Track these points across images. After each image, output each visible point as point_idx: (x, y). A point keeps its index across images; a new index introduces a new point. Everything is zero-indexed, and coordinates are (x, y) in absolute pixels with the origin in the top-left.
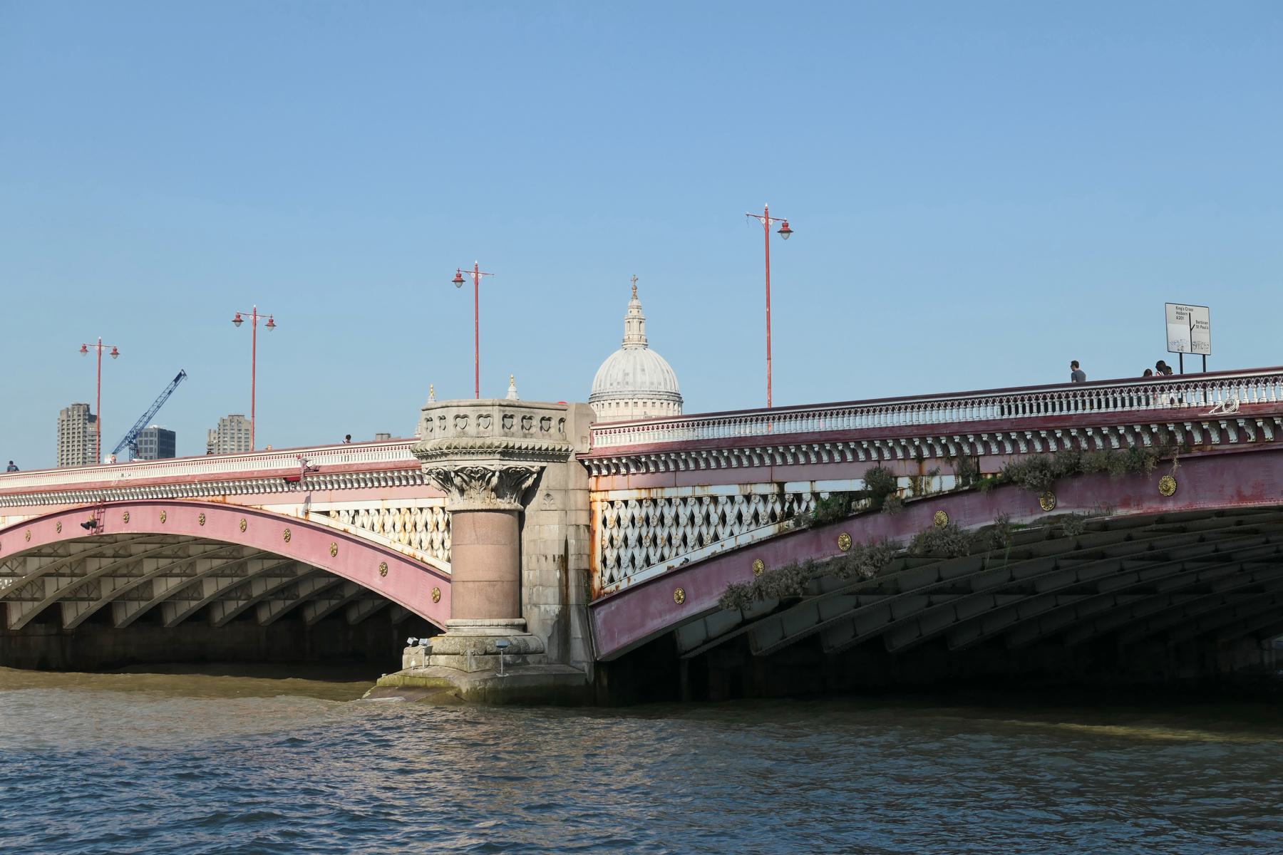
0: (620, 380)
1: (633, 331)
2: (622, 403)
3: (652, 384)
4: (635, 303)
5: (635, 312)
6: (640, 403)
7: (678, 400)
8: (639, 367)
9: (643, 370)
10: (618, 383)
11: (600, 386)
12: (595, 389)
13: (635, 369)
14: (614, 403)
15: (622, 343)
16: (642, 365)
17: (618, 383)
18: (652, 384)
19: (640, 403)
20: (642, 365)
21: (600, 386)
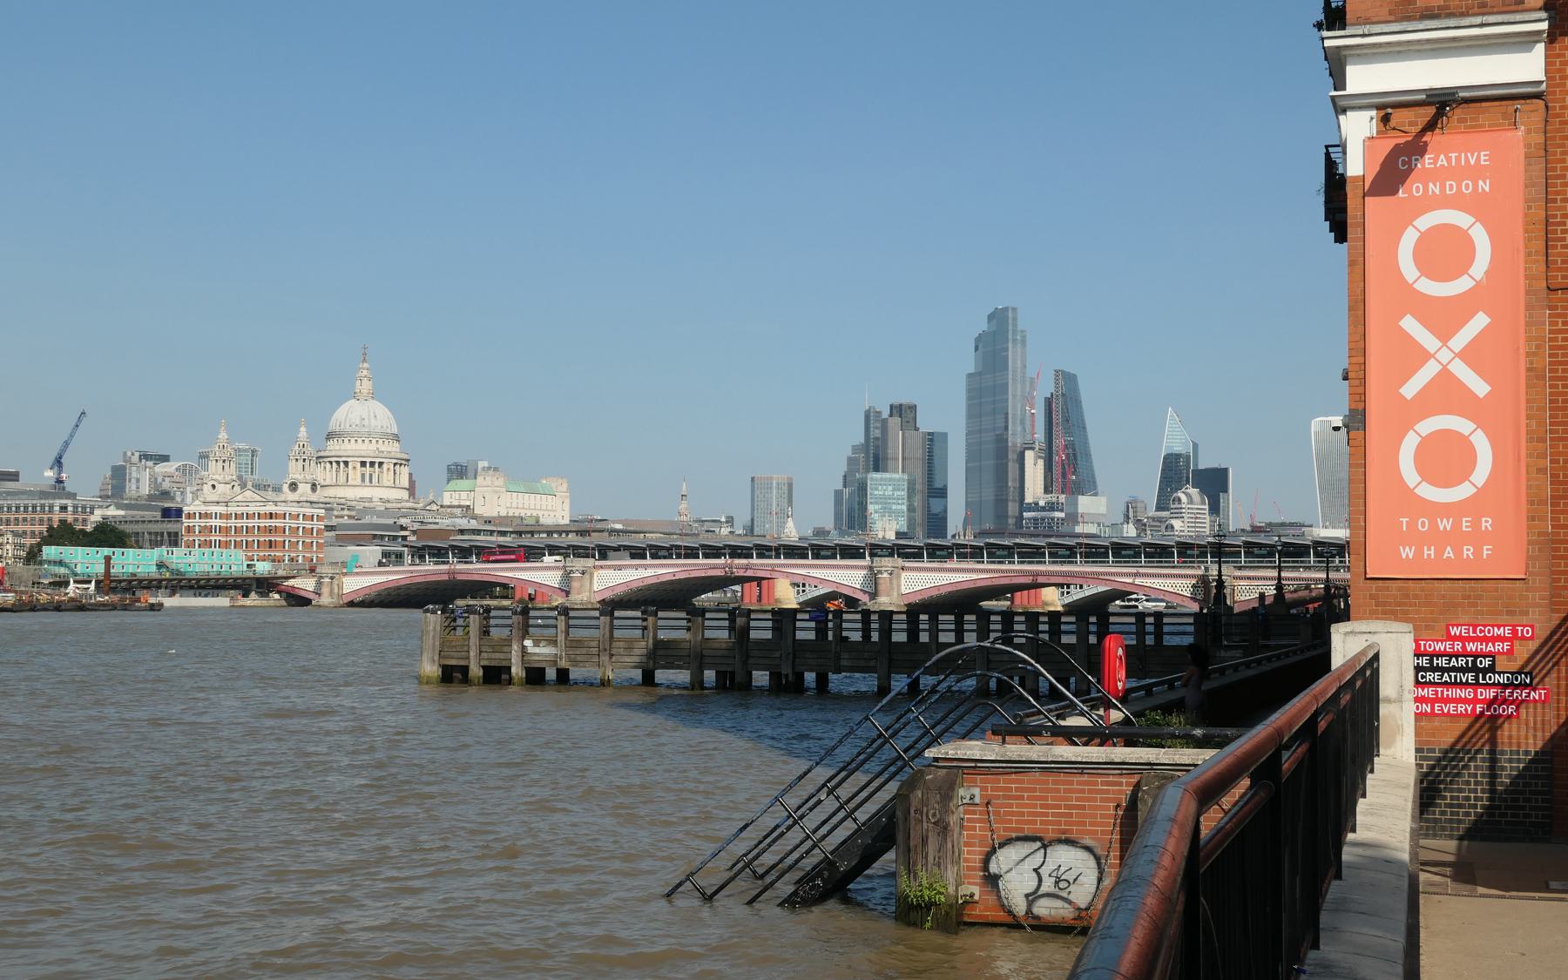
0: (358, 423)
1: (365, 386)
2: (360, 440)
3: (382, 427)
4: (366, 365)
5: (365, 372)
6: (374, 441)
7: (396, 438)
8: (372, 415)
9: (375, 417)
10: (356, 425)
11: (340, 426)
12: (333, 425)
13: (369, 416)
14: (353, 440)
15: (355, 396)
16: (374, 413)
17: (356, 425)
18: (382, 427)
19: (374, 441)
20: (374, 413)
21: (340, 426)
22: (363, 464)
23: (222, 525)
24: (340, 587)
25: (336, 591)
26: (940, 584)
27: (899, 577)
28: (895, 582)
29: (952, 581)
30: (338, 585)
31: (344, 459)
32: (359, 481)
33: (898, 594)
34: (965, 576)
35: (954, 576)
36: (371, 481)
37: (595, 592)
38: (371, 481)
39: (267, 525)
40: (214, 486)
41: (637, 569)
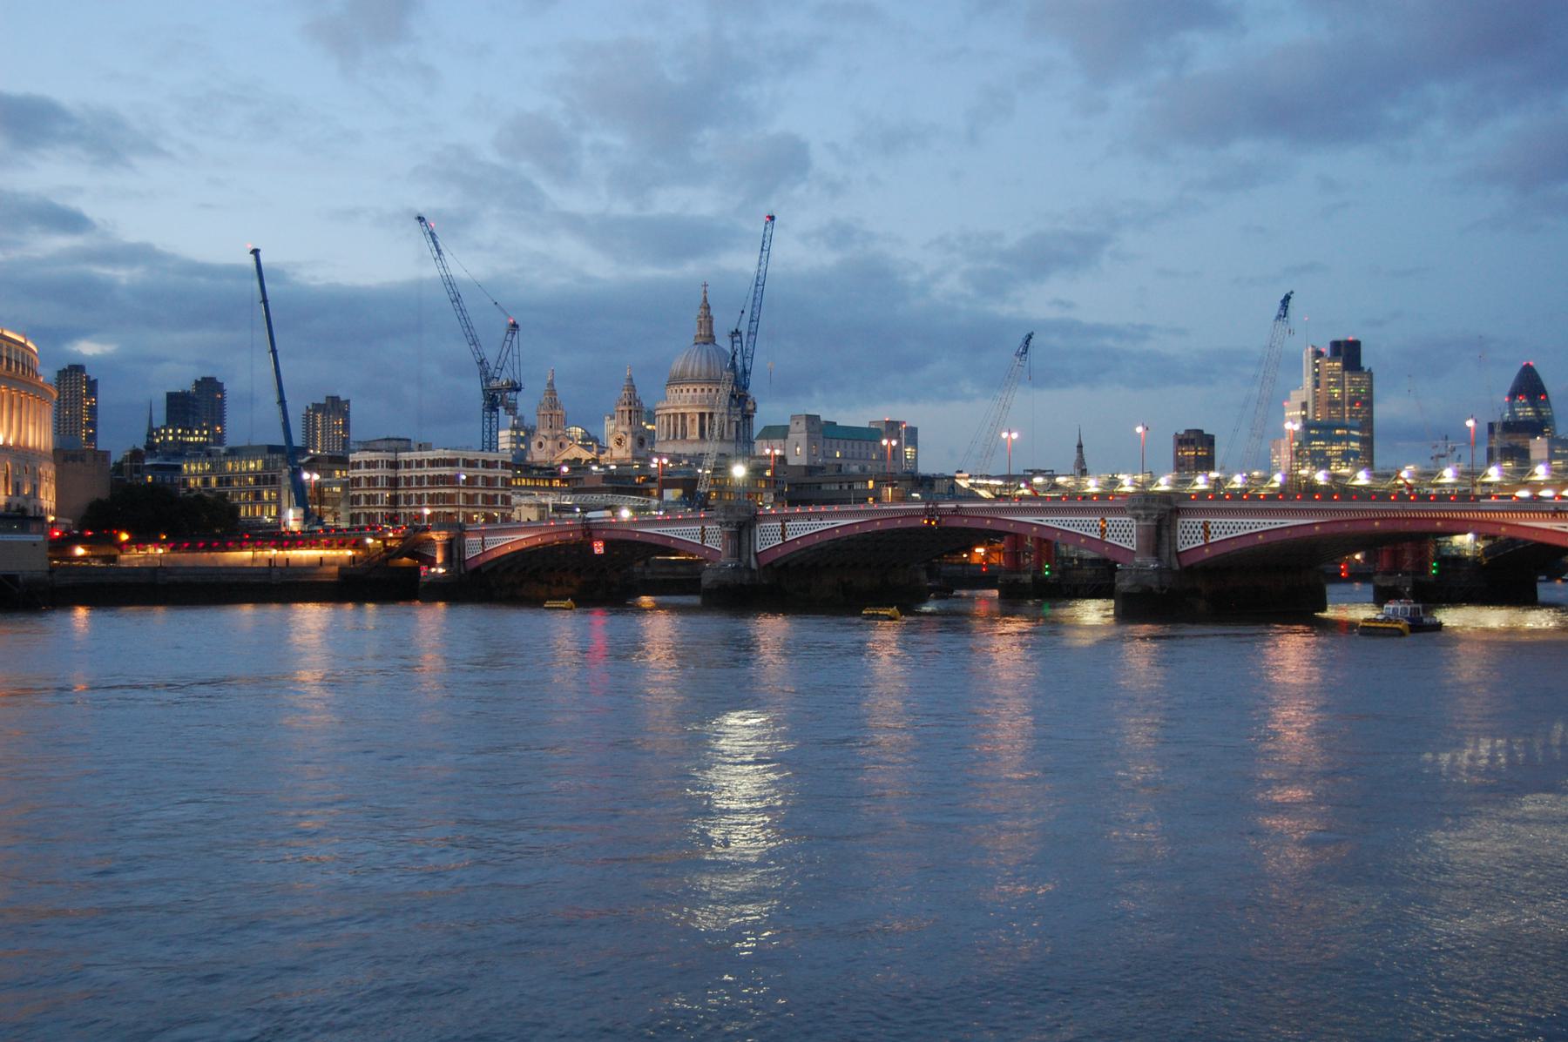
22: (702, 415)
23: (390, 475)
24: (462, 551)
25: (456, 556)
26: (1234, 535)
27: (1172, 526)
28: (1165, 532)
29: (1254, 530)
30: (459, 548)
31: (682, 410)
32: (697, 436)
33: (1170, 553)
34: (1273, 521)
35: (1256, 521)
36: (711, 436)
37: (756, 554)
38: (711, 436)
39: (437, 473)
40: (541, 445)
41: (809, 520)
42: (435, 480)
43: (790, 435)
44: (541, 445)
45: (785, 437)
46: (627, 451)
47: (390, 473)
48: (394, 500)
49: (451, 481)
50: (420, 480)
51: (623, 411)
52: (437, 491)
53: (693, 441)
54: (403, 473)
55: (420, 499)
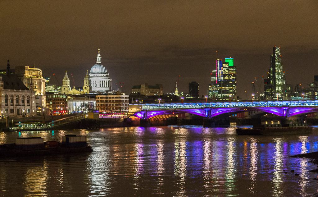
22: (100, 81)
24: (146, 115)
40: (64, 89)
42: (116, 101)
43: (141, 88)
44: (64, 89)
45: (140, 88)
46: (88, 91)
47: (106, 100)
48: (107, 105)
49: (120, 101)
50: (113, 101)
51: (86, 81)
52: (117, 103)
53: (98, 88)
54: (109, 99)
55: (110, 105)
